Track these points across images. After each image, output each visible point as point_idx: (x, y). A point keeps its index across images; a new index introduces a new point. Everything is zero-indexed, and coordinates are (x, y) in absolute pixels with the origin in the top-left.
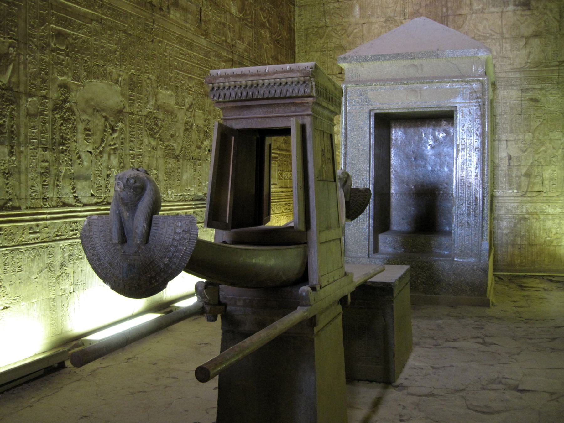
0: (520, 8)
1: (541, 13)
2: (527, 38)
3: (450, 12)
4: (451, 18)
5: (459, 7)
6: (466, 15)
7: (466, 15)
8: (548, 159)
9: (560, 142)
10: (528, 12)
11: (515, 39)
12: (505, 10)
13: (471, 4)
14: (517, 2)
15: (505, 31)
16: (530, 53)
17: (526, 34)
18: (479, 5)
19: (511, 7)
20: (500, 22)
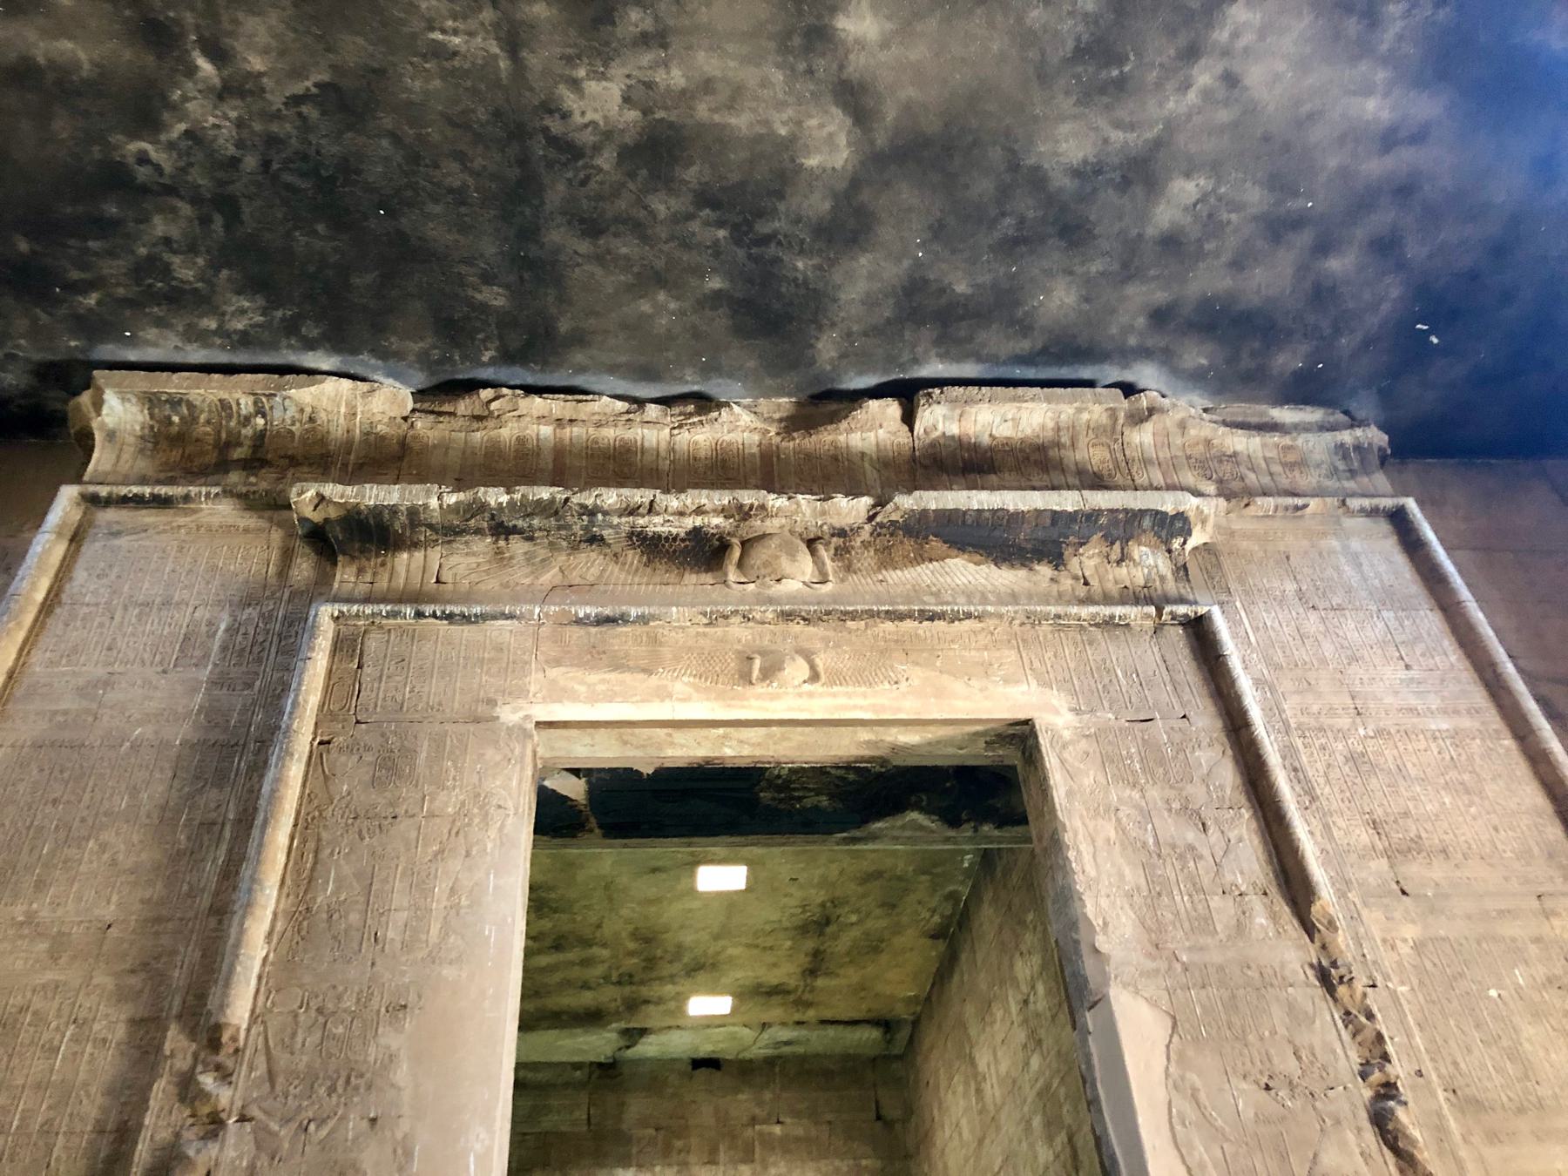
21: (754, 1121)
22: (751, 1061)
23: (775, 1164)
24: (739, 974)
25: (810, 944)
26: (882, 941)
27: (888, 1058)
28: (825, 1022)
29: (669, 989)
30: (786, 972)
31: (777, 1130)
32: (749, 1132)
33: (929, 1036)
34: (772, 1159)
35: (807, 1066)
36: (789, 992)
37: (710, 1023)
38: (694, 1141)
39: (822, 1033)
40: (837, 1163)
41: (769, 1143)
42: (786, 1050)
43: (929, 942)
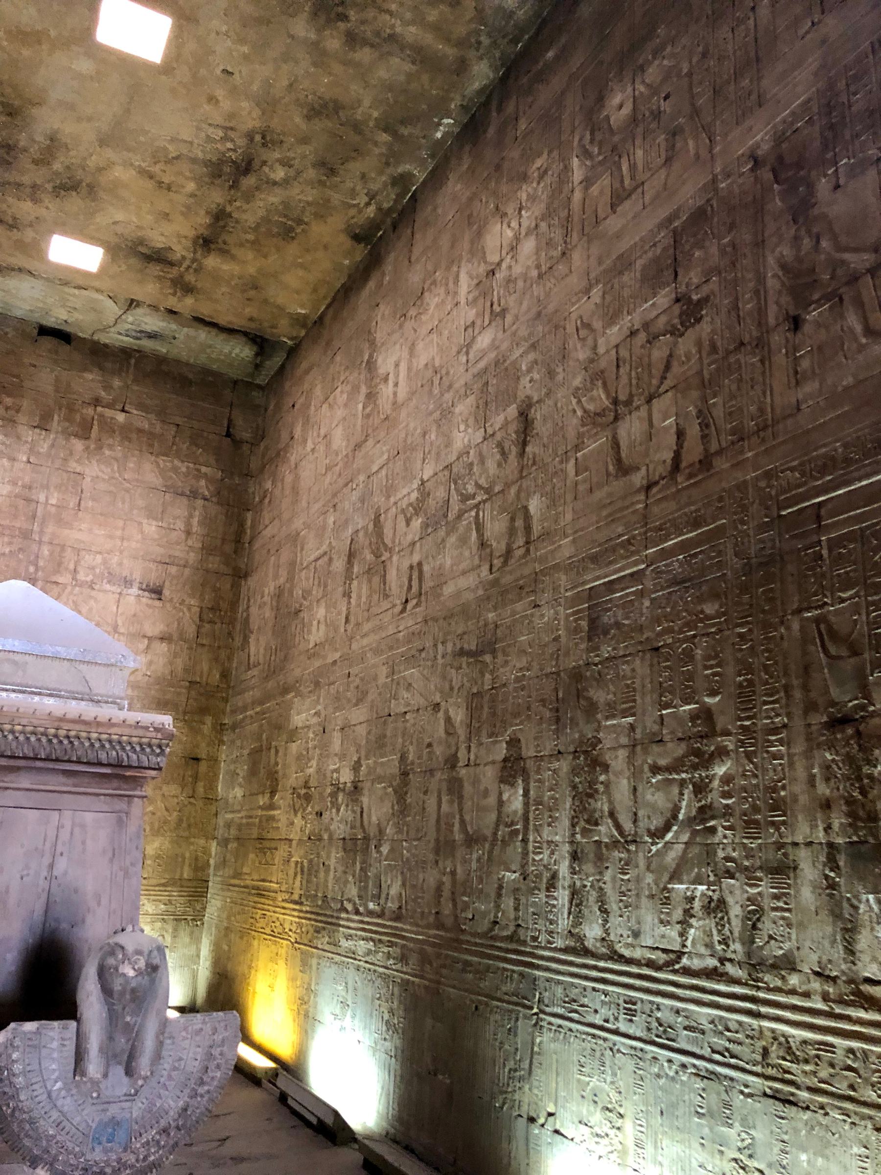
0: (146, 594)
1: (175, 608)
2: (150, 639)
3: (40, 573)
4: (40, 583)
5: (57, 571)
6: (65, 586)
7: (65, 586)
8: (156, 825)
9: (176, 800)
10: (158, 603)
11: (134, 637)
12: (124, 592)
13: (75, 571)
14: (144, 587)
15: (120, 622)
16: (150, 663)
17: (150, 634)
18: (87, 575)
19: (135, 591)
20: (115, 608)
21: (97, 402)
22: (106, 346)
23: (111, 447)
24: (120, 216)
25: (217, 197)
26: (299, 222)
27: (250, 385)
28: (200, 321)
29: (25, 208)
30: (173, 234)
31: (121, 417)
32: (90, 411)
33: (312, 356)
34: (110, 441)
35: (164, 368)
36: (171, 264)
37: (68, 279)
38: (25, 403)
39: (192, 332)
40: (177, 462)
41: (108, 427)
42: (148, 344)
43: (348, 243)
